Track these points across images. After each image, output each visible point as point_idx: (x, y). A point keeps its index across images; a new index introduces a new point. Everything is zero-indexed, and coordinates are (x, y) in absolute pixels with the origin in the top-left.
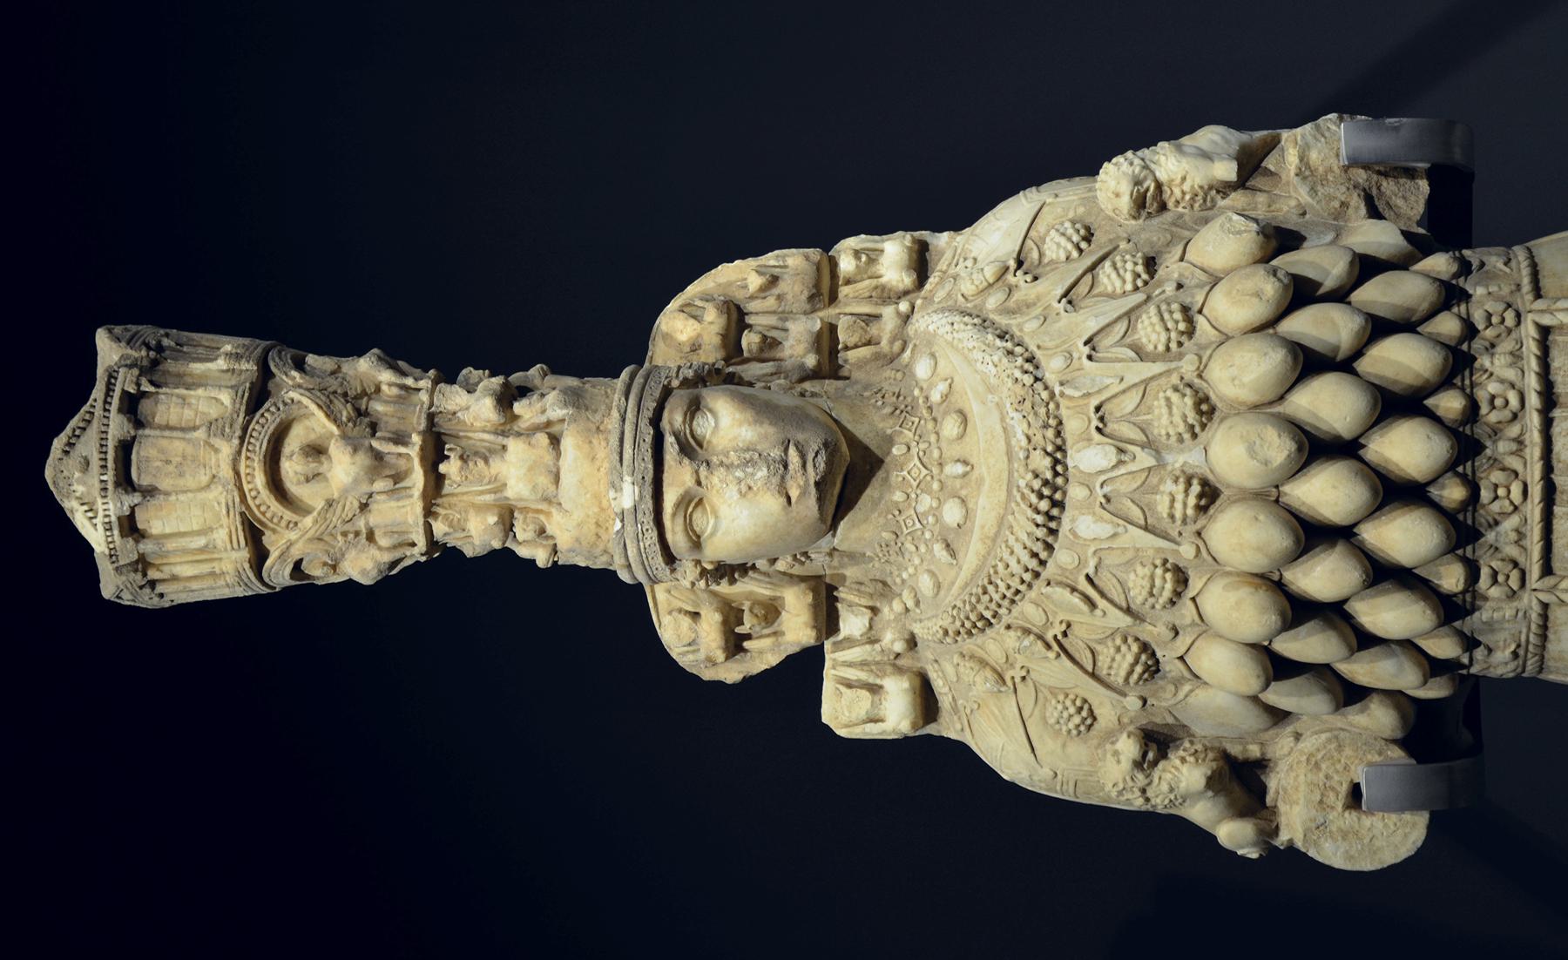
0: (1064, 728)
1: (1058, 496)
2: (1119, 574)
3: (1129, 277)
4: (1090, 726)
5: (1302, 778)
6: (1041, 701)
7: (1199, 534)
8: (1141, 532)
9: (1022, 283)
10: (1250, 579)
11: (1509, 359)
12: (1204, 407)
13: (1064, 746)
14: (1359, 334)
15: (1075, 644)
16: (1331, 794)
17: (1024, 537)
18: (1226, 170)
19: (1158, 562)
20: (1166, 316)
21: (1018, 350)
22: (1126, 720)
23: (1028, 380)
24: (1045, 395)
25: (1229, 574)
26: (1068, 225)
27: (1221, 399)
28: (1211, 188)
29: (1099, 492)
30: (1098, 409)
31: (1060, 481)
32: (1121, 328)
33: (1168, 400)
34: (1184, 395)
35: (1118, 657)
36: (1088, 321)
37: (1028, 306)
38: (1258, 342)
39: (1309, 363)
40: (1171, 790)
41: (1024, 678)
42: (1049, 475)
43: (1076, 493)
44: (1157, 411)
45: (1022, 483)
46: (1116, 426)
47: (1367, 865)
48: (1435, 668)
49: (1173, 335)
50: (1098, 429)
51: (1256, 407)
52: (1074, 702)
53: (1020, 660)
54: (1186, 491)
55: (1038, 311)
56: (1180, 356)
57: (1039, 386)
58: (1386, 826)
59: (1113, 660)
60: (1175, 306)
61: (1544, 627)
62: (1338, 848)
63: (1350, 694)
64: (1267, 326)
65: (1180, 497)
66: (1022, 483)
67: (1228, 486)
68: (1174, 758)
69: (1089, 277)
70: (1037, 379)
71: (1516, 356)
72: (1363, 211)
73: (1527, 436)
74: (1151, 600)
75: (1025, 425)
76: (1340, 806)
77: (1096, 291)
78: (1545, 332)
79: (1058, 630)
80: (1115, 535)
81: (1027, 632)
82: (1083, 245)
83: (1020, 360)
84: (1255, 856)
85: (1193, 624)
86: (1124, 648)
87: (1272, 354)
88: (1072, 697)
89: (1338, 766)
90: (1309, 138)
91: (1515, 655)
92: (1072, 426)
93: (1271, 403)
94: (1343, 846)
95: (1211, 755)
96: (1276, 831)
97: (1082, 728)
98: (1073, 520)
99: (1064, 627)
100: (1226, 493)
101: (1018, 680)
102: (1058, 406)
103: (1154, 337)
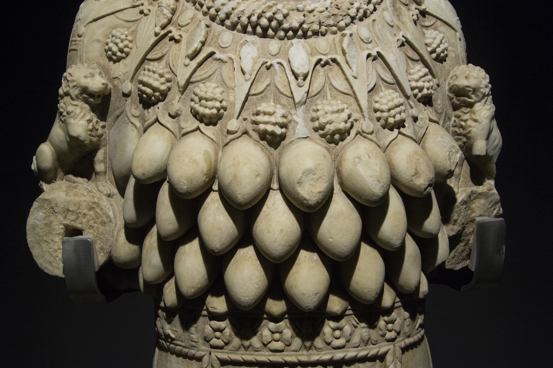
0: (109, 40)
1: (270, 32)
2: (215, 76)
3: (420, 84)
4: (110, 59)
5: (83, 199)
6: (126, 24)
7: (246, 133)
8: (246, 91)
9: (412, 13)
10: (212, 170)
11: (366, 338)
12: (337, 136)
13: (98, 41)
14: (387, 243)
15: (166, 46)
16: (74, 217)
17: (241, 8)
18: (480, 147)
19: (224, 104)
20: (398, 110)
21: (371, 7)
22: (116, 82)
23: (352, 12)
24: (342, 24)
25: (217, 154)
26: (446, 45)
27: (343, 148)
28: (468, 138)
29: (274, 61)
30: (334, 60)
31: (282, 33)
32: (389, 78)
33: (343, 110)
34: (346, 122)
35: (156, 76)
36: (394, 56)
37: (398, 16)
38: (386, 178)
39: (371, 212)
40: (68, 113)
41: (142, 12)
42: (286, 25)
43: (274, 45)
44: (334, 102)
45: (280, 6)
46: (322, 73)
47: (30, 239)
48: (156, 288)
49: (386, 114)
50: (320, 60)
51: (339, 172)
52: (126, 46)
53: (154, 9)
54: (275, 124)
55: (396, 22)
56: (371, 119)
57: (348, 20)
58: (56, 251)
59: (154, 72)
60: (403, 115)
61: (185, 356)
62: (40, 221)
63: (136, 233)
64: (394, 181)
65: (273, 119)
66: (280, 6)
67: (281, 154)
68: (90, 115)
69: (417, 57)
70: (353, 18)
71: (366, 342)
72: (452, 234)
73: (315, 352)
74: (197, 99)
75: (321, 9)
76: (67, 222)
77: (409, 61)
78: (381, 358)
79: (175, 34)
80: (243, 73)
81: (173, 12)
82: (434, 55)
83: (365, 7)
84: (33, 167)
85: (181, 128)
86: (163, 80)
87: (379, 186)
88: (130, 45)
89: (92, 222)
90: (492, 198)
91: (168, 336)
92: (321, 43)
93: (342, 184)
94: (41, 224)
95: (94, 139)
96: (49, 182)
97: (109, 53)
98: (253, 43)
99: (177, 37)
100: (275, 152)
101: (141, 8)
102: (335, 33)
103: (384, 101)
